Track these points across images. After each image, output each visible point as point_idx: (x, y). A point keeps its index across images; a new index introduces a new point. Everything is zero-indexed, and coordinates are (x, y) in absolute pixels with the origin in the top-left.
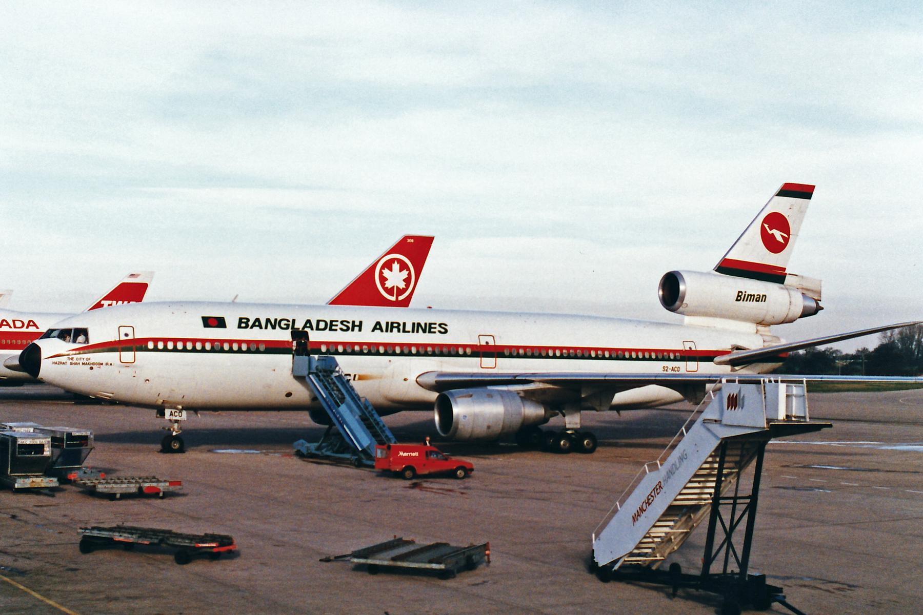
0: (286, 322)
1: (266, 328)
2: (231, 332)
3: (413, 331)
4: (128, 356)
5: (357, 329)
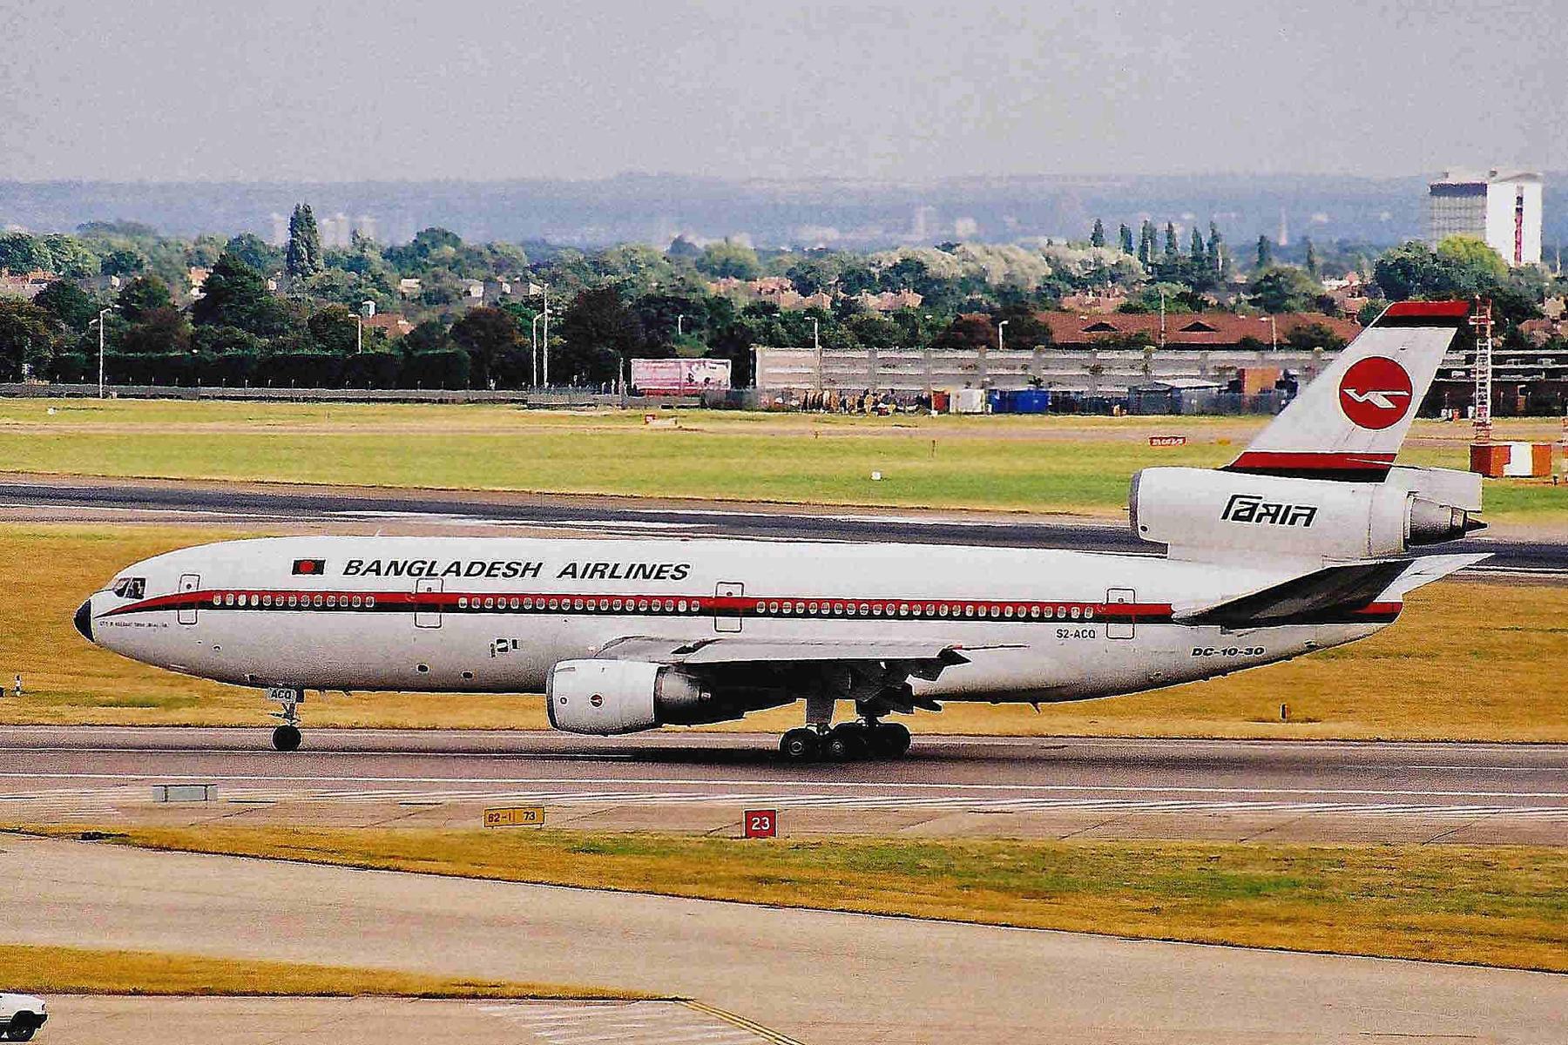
0: (420, 565)
1: (387, 574)
2: (332, 580)
3: (627, 576)
4: (187, 615)
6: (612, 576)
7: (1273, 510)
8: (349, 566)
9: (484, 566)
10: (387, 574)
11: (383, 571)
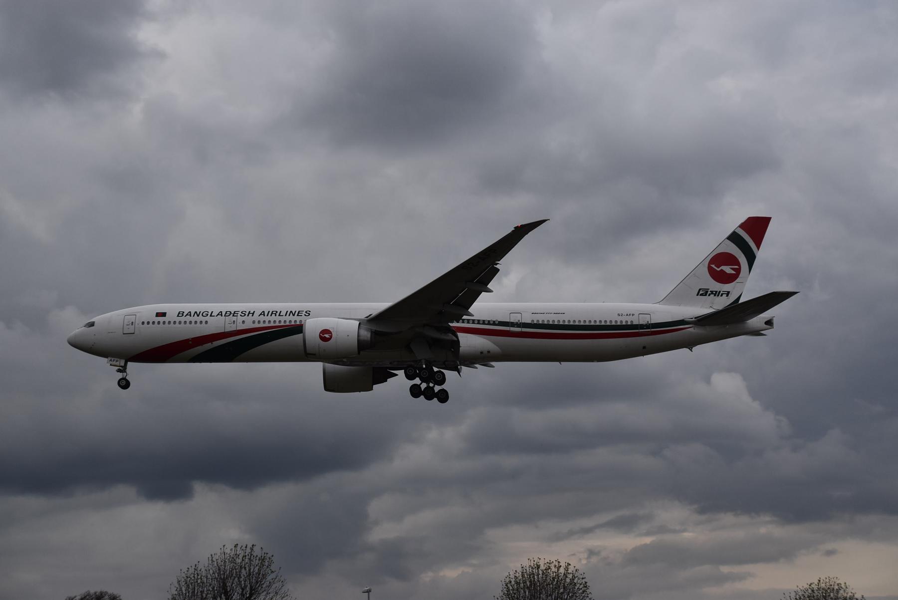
0: (207, 313)
1: (194, 316)
3: (286, 315)
5: (251, 315)
6: (279, 315)
7: (714, 293)
8: (179, 313)
9: (230, 312)
10: (194, 316)
11: (192, 315)
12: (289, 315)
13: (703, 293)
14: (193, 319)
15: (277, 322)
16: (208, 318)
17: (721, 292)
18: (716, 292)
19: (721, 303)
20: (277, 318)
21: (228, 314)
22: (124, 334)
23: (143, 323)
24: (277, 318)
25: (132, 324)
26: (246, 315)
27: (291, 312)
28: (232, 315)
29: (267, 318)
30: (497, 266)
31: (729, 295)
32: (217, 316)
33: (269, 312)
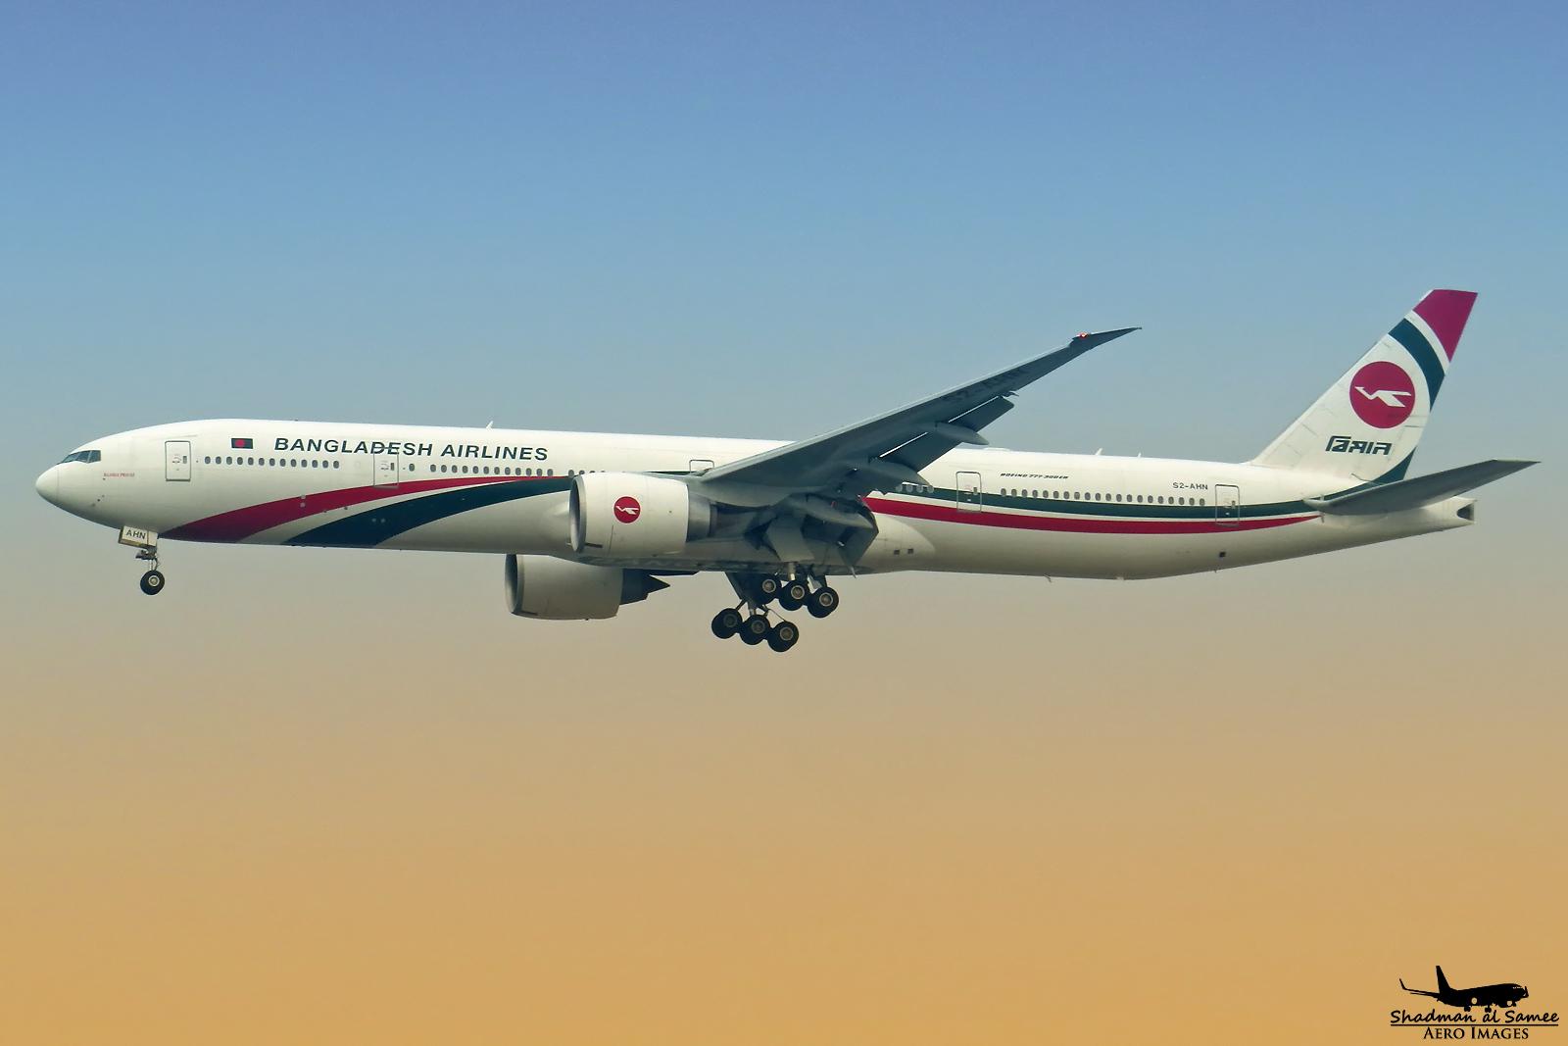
0: (334, 444)
3: (497, 457)
6: (484, 456)
7: (1361, 445)
8: (278, 444)
9: (383, 445)
12: (504, 457)
13: (1340, 445)
14: (311, 455)
15: (481, 470)
16: (338, 455)
17: (1375, 445)
18: (1365, 443)
19: (1375, 467)
20: (481, 462)
21: (378, 447)
22: (167, 480)
23: (208, 460)
24: (481, 462)
25: (185, 462)
26: (417, 452)
27: (506, 449)
28: (386, 451)
29: (460, 461)
30: (1010, 399)
31: (1390, 452)
32: (356, 452)
33: (461, 447)
